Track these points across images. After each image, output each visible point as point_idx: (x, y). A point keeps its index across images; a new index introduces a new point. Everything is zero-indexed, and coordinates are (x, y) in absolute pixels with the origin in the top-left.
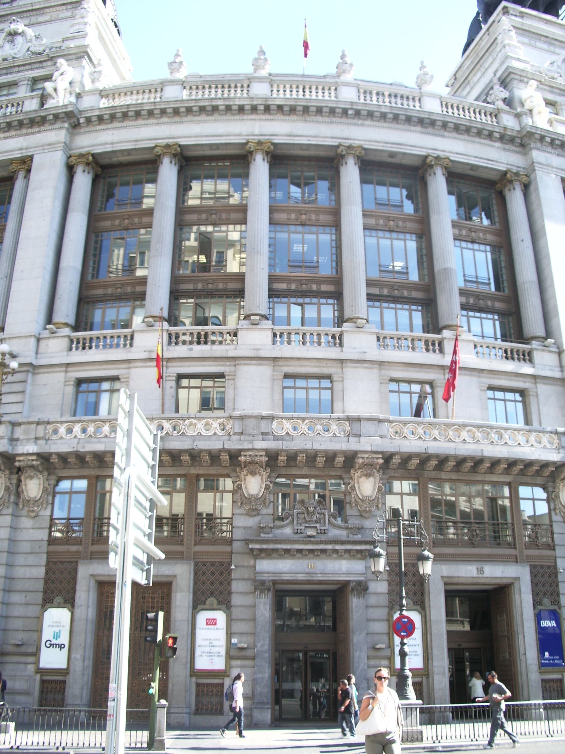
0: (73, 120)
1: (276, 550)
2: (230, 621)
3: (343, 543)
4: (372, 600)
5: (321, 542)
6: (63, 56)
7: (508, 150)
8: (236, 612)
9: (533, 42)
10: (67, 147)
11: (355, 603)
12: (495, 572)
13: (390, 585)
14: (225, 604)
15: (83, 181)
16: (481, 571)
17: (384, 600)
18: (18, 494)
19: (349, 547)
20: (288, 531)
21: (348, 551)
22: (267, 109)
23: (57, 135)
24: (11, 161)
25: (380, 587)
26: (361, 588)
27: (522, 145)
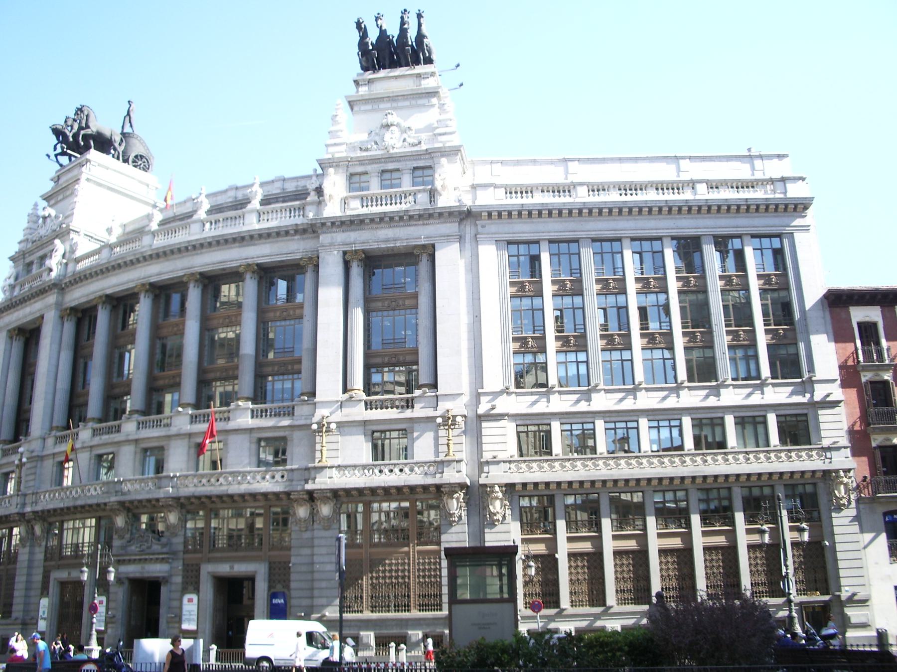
0: (61, 286)
3: (159, 554)
4: (173, 588)
5: (148, 554)
6: (57, 237)
7: (307, 238)
8: (112, 596)
9: (376, 107)
10: (58, 304)
11: (164, 590)
12: (241, 569)
13: (183, 577)
15: (69, 327)
16: (232, 568)
17: (179, 587)
18: (33, 534)
19: (157, 556)
20: (133, 548)
21: (157, 559)
22: (145, 258)
24: (37, 319)
25: (178, 579)
26: (166, 580)
27: (314, 232)
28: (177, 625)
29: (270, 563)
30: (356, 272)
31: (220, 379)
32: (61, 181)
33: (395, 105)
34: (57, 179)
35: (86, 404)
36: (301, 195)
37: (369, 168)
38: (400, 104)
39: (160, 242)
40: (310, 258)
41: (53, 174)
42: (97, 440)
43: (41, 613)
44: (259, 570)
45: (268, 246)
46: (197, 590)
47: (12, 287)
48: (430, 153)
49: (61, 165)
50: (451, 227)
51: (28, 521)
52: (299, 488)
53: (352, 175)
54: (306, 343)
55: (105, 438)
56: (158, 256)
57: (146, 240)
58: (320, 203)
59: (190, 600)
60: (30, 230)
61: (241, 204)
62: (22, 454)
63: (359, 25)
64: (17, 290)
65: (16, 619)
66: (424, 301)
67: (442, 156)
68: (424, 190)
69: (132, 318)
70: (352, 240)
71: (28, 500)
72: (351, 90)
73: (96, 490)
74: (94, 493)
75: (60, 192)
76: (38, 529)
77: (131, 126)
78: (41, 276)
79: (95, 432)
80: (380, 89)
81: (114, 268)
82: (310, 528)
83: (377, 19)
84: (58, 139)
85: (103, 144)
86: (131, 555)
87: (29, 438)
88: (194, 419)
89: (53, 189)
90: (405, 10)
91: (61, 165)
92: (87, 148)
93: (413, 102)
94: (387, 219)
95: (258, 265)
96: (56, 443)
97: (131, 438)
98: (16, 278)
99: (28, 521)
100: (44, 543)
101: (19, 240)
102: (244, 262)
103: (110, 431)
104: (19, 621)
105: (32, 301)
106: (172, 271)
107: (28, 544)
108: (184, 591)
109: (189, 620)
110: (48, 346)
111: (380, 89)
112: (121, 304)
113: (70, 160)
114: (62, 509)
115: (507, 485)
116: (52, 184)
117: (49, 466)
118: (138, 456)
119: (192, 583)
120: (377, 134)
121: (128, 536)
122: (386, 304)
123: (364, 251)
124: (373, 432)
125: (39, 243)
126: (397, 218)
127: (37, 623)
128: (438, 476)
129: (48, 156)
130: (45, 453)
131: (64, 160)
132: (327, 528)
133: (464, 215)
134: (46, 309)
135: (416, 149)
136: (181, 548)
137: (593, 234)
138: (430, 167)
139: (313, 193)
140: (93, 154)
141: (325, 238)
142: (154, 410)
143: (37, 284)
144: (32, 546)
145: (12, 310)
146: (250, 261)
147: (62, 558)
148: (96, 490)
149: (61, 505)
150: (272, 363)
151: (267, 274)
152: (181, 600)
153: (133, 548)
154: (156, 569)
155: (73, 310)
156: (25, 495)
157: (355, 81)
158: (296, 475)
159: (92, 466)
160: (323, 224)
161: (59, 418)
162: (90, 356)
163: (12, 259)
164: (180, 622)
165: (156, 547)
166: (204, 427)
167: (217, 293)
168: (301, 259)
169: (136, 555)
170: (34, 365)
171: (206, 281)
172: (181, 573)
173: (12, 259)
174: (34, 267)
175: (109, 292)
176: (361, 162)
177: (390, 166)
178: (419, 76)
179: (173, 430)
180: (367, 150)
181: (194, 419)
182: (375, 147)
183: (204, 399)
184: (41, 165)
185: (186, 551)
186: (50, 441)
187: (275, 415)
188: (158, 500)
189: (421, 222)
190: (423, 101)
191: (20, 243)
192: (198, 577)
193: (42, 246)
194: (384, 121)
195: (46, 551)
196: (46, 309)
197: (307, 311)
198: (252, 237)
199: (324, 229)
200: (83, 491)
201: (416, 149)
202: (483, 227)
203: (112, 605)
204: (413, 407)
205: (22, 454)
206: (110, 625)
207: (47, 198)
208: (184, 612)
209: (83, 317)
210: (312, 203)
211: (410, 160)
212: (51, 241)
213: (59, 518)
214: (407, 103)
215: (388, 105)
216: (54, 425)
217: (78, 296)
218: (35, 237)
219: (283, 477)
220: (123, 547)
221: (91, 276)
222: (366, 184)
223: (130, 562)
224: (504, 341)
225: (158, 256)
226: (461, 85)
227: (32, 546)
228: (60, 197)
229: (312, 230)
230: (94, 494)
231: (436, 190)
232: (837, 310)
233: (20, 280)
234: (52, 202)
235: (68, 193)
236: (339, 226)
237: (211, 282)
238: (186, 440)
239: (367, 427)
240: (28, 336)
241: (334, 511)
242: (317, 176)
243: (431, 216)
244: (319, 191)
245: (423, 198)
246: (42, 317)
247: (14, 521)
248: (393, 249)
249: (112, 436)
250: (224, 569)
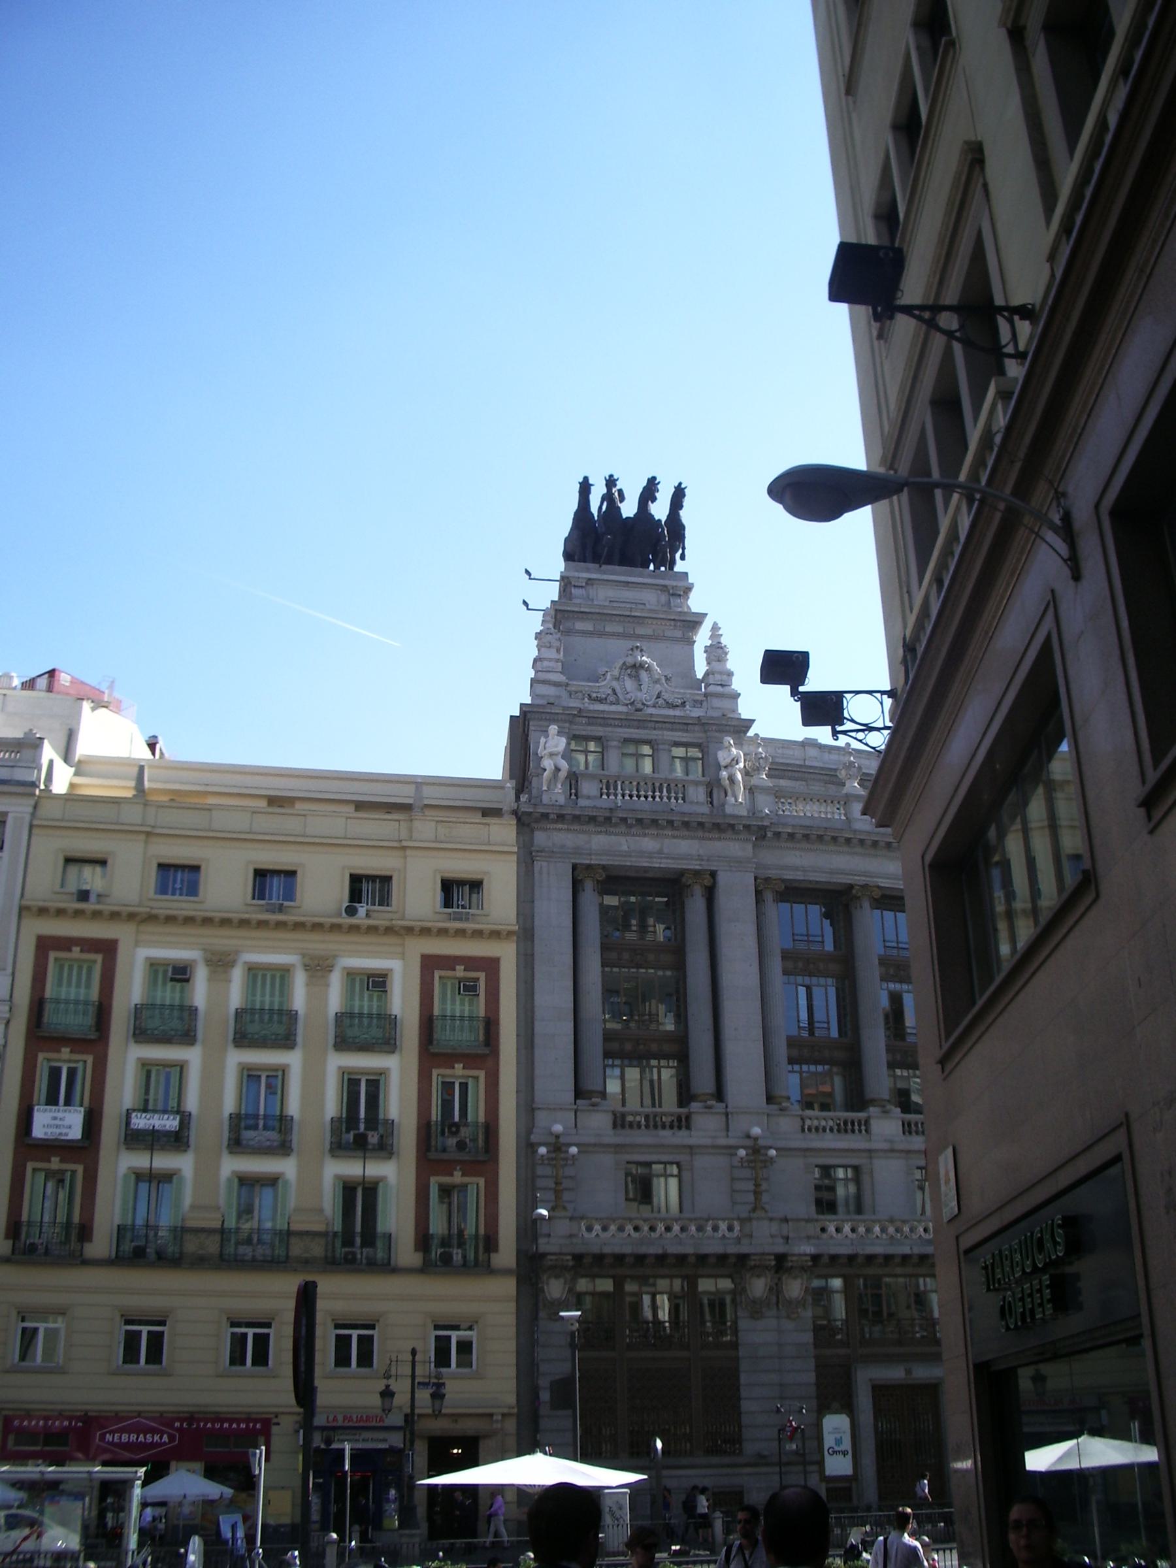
80: (603, 595)
111: (603, 595)
122: (626, 956)
123: (604, 867)
128: (745, 1241)
135: (677, 712)
160: (545, 816)
176: (594, 719)
180: (601, 701)
182: (612, 698)
194: (630, 661)
201: (677, 712)
204: (688, 1127)
243: (717, 827)
245: (698, 794)
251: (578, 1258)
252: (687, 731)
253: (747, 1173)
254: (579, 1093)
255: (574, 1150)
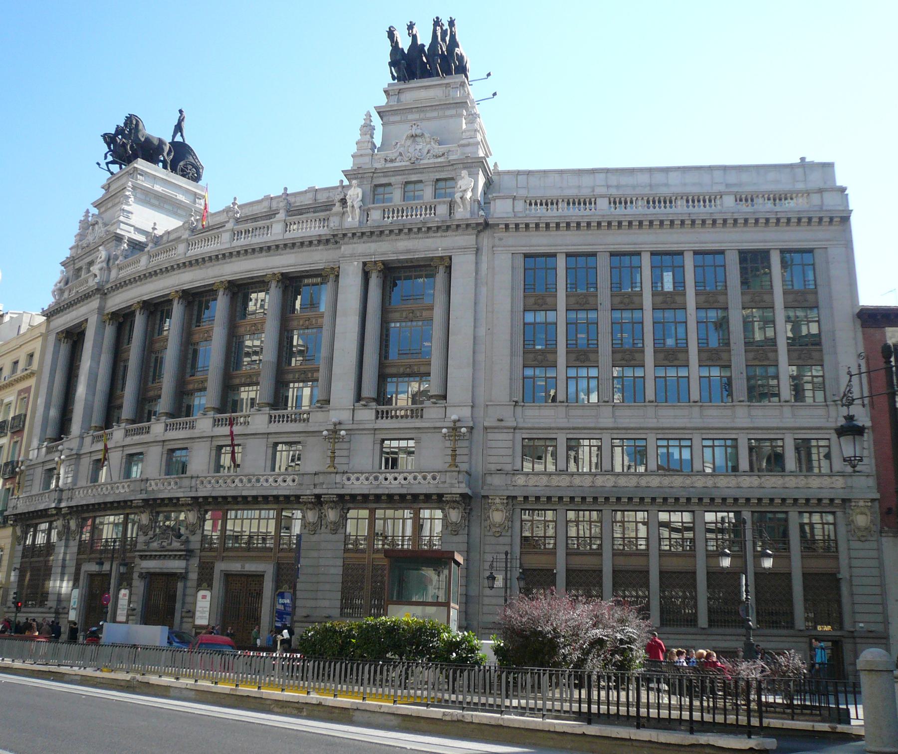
0: (102, 292)
1: (151, 555)
2: (131, 594)
10: (101, 309)
12: (251, 567)
14: (130, 586)
15: (109, 331)
16: (243, 567)
17: (195, 584)
18: (69, 528)
23: (95, 303)
25: (193, 576)
26: (183, 577)
28: (190, 620)
29: (278, 564)
30: (375, 282)
31: (245, 385)
32: (112, 188)
33: (422, 115)
34: (107, 187)
35: (120, 407)
36: (327, 207)
37: (392, 180)
38: (429, 115)
39: (181, 252)
40: (333, 269)
41: (104, 182)
42: (129, 440)
43: (72, 604)
44: (267, 569)
45: (293, 255)
46: (210, 587)
47: (61, 291)
48: (452, 165)
49: (112, 173)
50: (468, 239)
51: (64, 516)
52: (308, 492)
53: (376, 186)
54: (324, 352)
55: (137, 438)
56: (191, 264)
57: (181, 248)
58: (344, 213)
59: (204, 597)
60: (81, 236)
61: (271, 214)
62: (61, 451)
63: (391, 34)
64: (66, 295)
65: (51, 608)
66: (438, 314)
67: (464, 168)
68: (444, 202)
69: (167, 324)
70: (372, 251)
71: (65, 495)
72: (382, 100)
73: (123, 487)
74: (122, 491)
75: (111, 199)
76: (73, 524)
77: (182, 135)
78: (87, 282)
79: (127, 433)
80: (408, 98)
81: (150, 275)
82: (318, 531)
83: (411, 27)
84: (109, 148)
85: (150, 151)
86: (153, 551)
87: (70, 437)
88: (216, 422)
89: (104, 196)
90: (437, 18)
91: (112, 173)
92: (135, 157)
93: (441, 113)
94: (406, 231)
95: (282, 274)
96: (93, 442)
97: (158, 439)
98: (67, 283)
99: (64, 516)
100: (78, 538)
101: (71, 246)
102: (270, 271)
103: (139, 432)
104: (53, 610)
105: (78, 305)
106: (204, 279)
107: (64, 538)
108: (199, 587)
109: (202, 618)
110: (91, 349)
112: (157, 309)
113: (121, 168)
114: (93, 505)
115: (508, 497)
116: (103, 191)
117: (86, 464)
118: (165, 456)
119: (205, 580)
120: (402, 146)
121: (151, 533)
122: (404, 315)
123: (383, 262)
124: (383, 440)
125: (88, 250)
126: (416, 230)
127: (68, 613)
128: (441, 485)
129: (98, 164)
130: (82, 452)
131: (115, 168)
132: (335, 531)
133: (481, 228)
134: (88, 311)
136: (198, 546)
137: (612, 248)
138: (452, 179)
139: (338, 204)
140: (141, 164)
141: (346, 249)
142: (183, 414)
143: (82, 289)
144: (67, 540)
145: (61, 314)
146: (276, 271)
147: (92, 551)
148: (123, 487)
149: (93, 502)
150: (294, 371)
151: (291, 284)
152: (195, 596)
153: (155, 545)
154: (176, 565)
155: (114, 315)
156: (62, 490)
157: (385, 92)
158: (307, 480)
159: (123, 466)
160: (345, 235)
161: (97, 419)
162: (127, 360)
163: (63, 264)
164: (193, 617)
165: (176, 544)
166: (226, 430)
167: (246, 300)
168: (323, 269)
169: (156, 551)
170: (78, 367)
171: (236, 289)
172: (197, 569)
173: (63, 264)
174: (83, 272)
175: (145, 298)
176: (386, 173)
177: (414, 178)
178: (447, 85)
179: (195, 433)
180: (392, 161)
181: (216, 422)
183: (230, 404)
184: (91, 171)
185: (203, 549)
186: (88, 440)
187: (291, 421)
188: (178, 499)
189: (439, 234)
190: (452, 112)
191: (71, 249)
192: (212, 574)
193: (89, 253)
195: (80, 545)
196: (88, 311)
197: (326, 321)
198: (277, 246)
199: (346, 239)
200: (112, 488)
201: (439, 160)
202: (500, 239)
203: (134, 598)
205: (61, 451)
206: (131, 618)
207: (97, 205)
208: (198, 609)
209: (122, 320)
210: (336, 214)
211: (432, 172)
212: (96, 249)
213: (91, 514)
214: (435, 114)
215: (416, 116)
216: (93, 425)
217: (118, 301)
218: (84, 243)
219: (294, 481)
220: (147, 543)
221: (130, 282)
222: (421, 193)
223: (151, 557)
224: (512, 354)
225: (191, 264)
226: (495, 94)
227: (67, 540)
228: (110, 205)
229: (333, 240)
230: (123, 492)
231: (455, 202)
232: (872, 330)
233: (70, 284)
234: (103, 209)
235: (117, 200)
236: (360, 237)
237: (239, 290)
238: (209, 443)
239: (377, 436)
240: (74, 337)
241: (341, 516)
242: (343, 187)
244: (343, 201)
245: (442, 210)
246: (86, 320)
247: (53, 515)
248: (411, 260)
249: (142, 436)
250: (235, 567)
251: (341, 497)
252: (443, 171)
253: (448, 444)
254: (359, 398)
255: (343, 433)
